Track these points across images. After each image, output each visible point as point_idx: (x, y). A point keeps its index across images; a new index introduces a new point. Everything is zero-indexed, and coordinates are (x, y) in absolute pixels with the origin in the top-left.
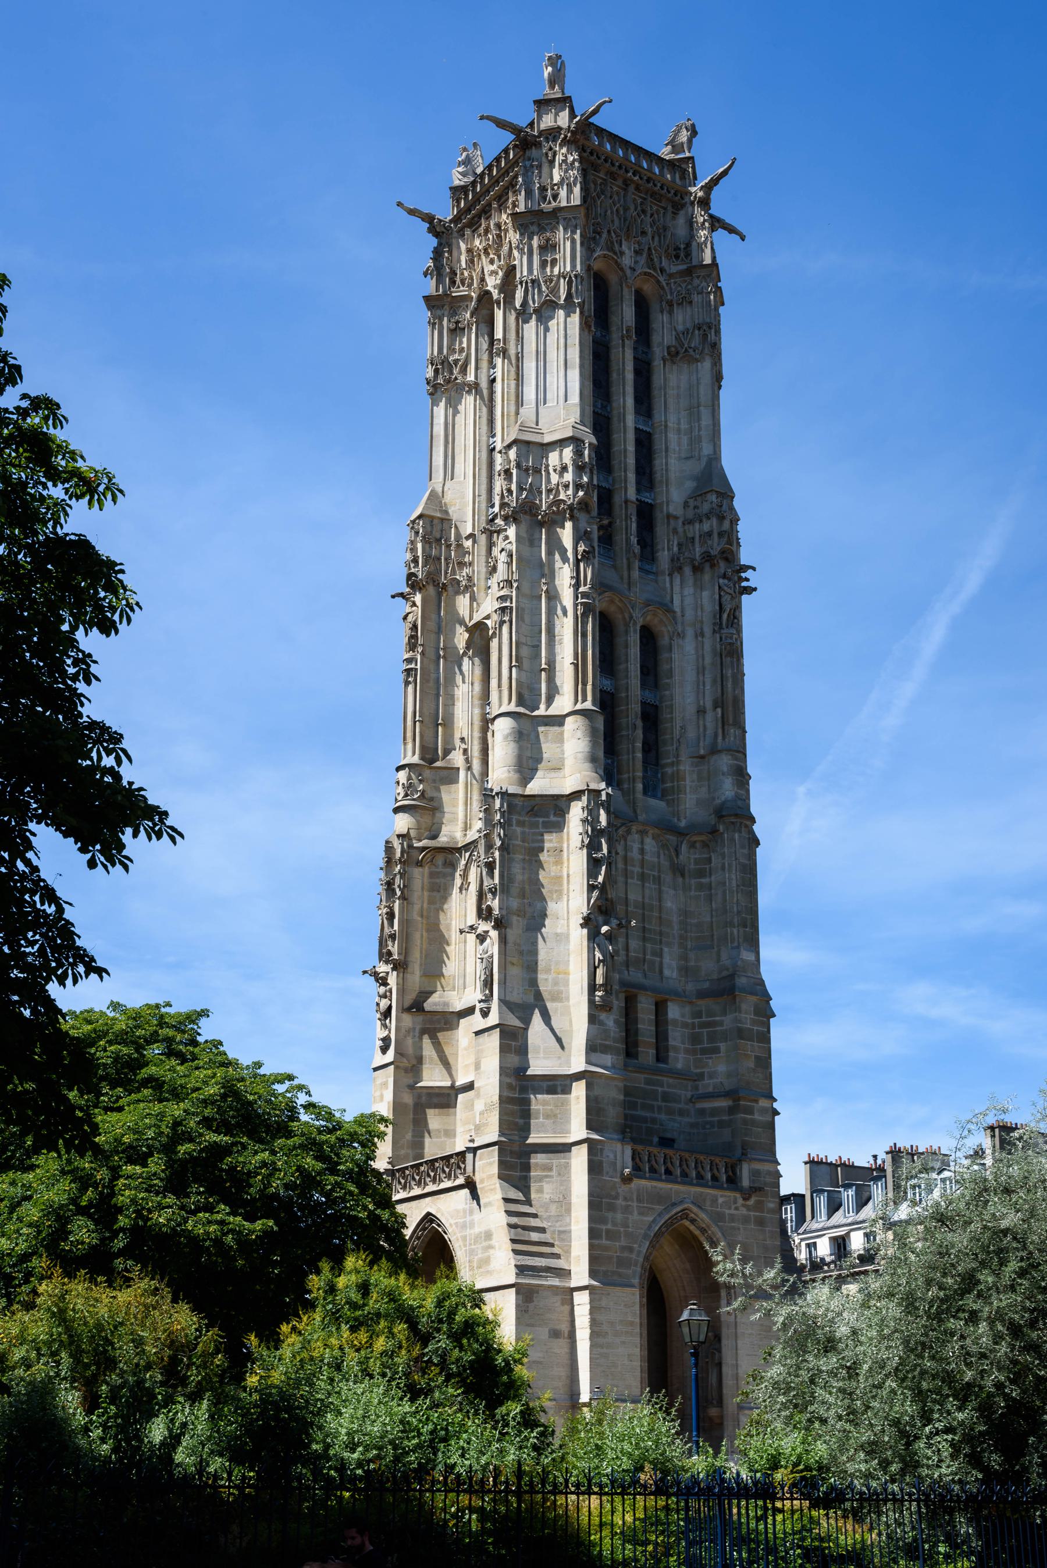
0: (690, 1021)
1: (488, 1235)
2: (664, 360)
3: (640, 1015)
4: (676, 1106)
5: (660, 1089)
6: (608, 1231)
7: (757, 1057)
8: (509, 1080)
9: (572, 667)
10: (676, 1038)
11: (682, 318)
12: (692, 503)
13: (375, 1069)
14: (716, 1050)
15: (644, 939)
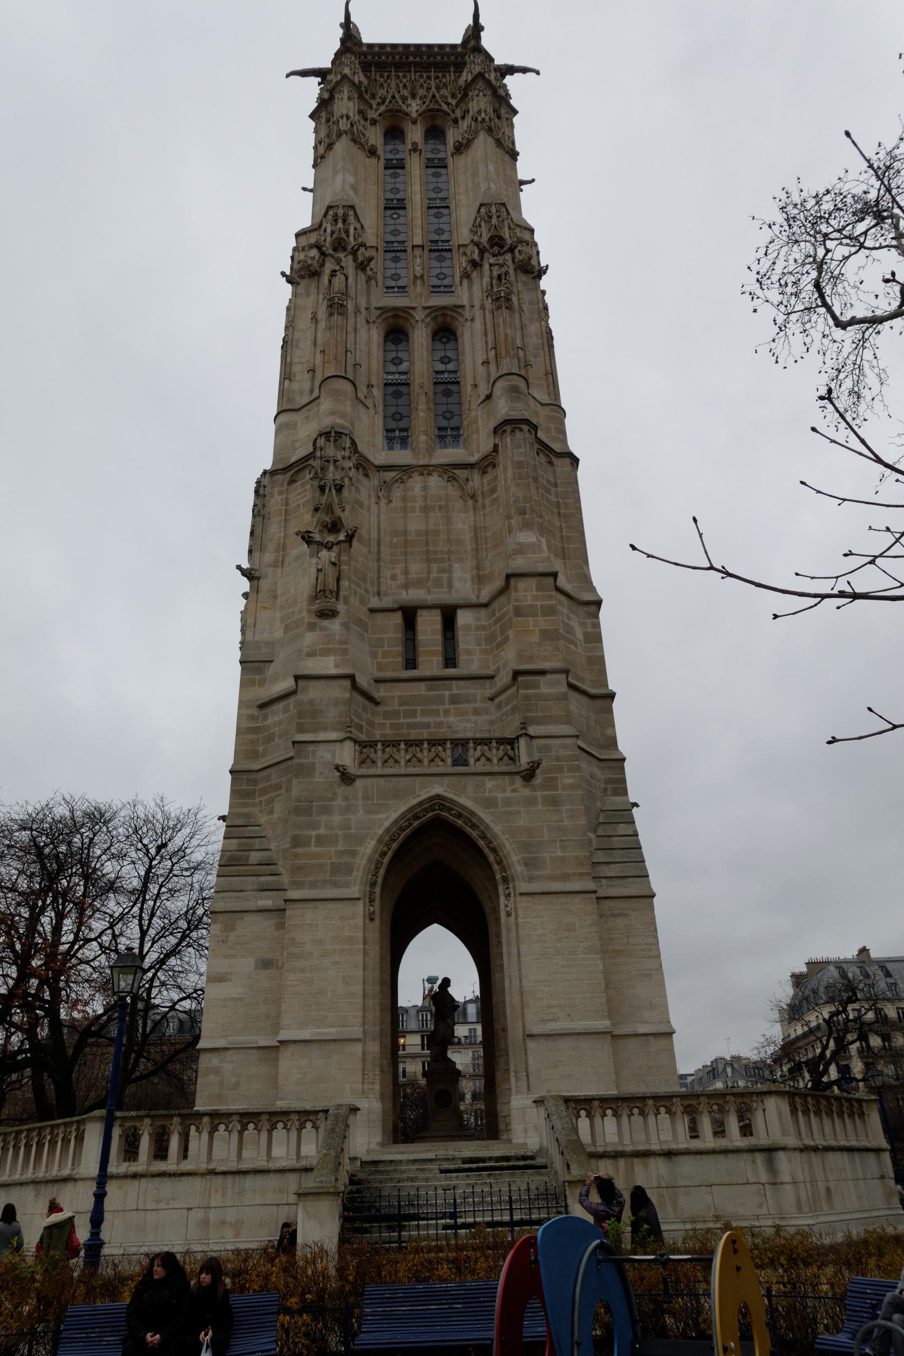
0: (486, 623)
2: (452, 155)
4: (470, 706)
5: (447, 693)
7: (540, 631)
8: (250, 712)
10: (466, 641)
14: (506, 640)
15: (428, 561)
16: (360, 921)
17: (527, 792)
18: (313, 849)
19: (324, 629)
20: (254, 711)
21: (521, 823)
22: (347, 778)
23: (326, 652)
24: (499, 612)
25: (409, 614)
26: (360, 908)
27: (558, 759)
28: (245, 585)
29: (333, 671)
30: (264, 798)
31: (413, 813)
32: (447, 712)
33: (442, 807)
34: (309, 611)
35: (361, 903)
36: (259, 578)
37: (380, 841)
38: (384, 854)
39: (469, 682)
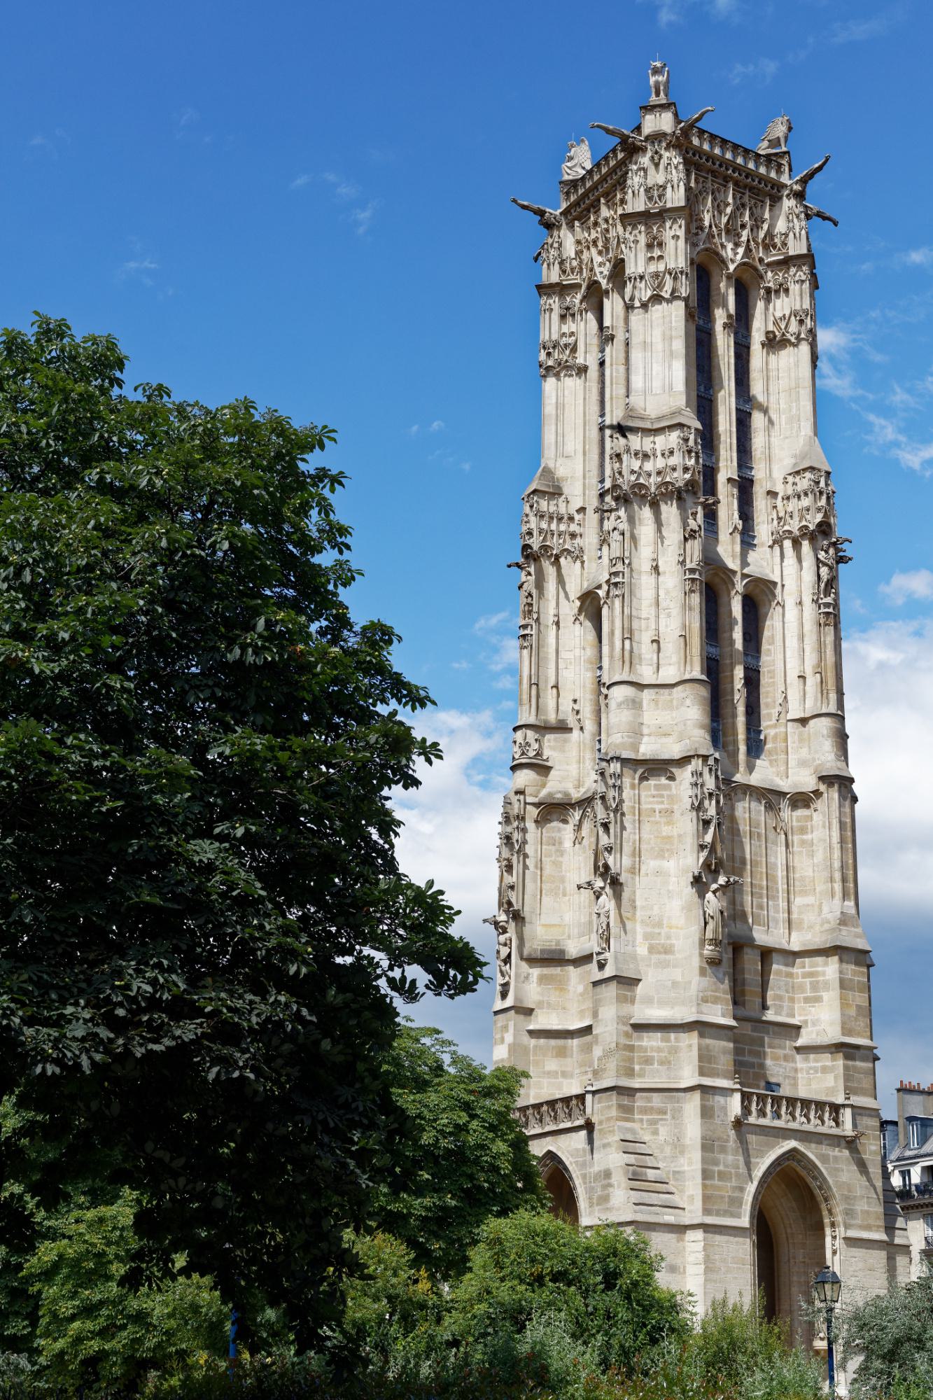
1: (607, 1174)
2: (763, 345)
3: (747, 966)
6: (720, 1173)
9: (682, 639)
11: (782, 306)
12: (790, 479)
13: (496, 1013)
14: (818, 999)
20: (629, 1029)
23: (716, 1000)
24: (811, 967)
30: (645, 1117)
34: (701, 955)
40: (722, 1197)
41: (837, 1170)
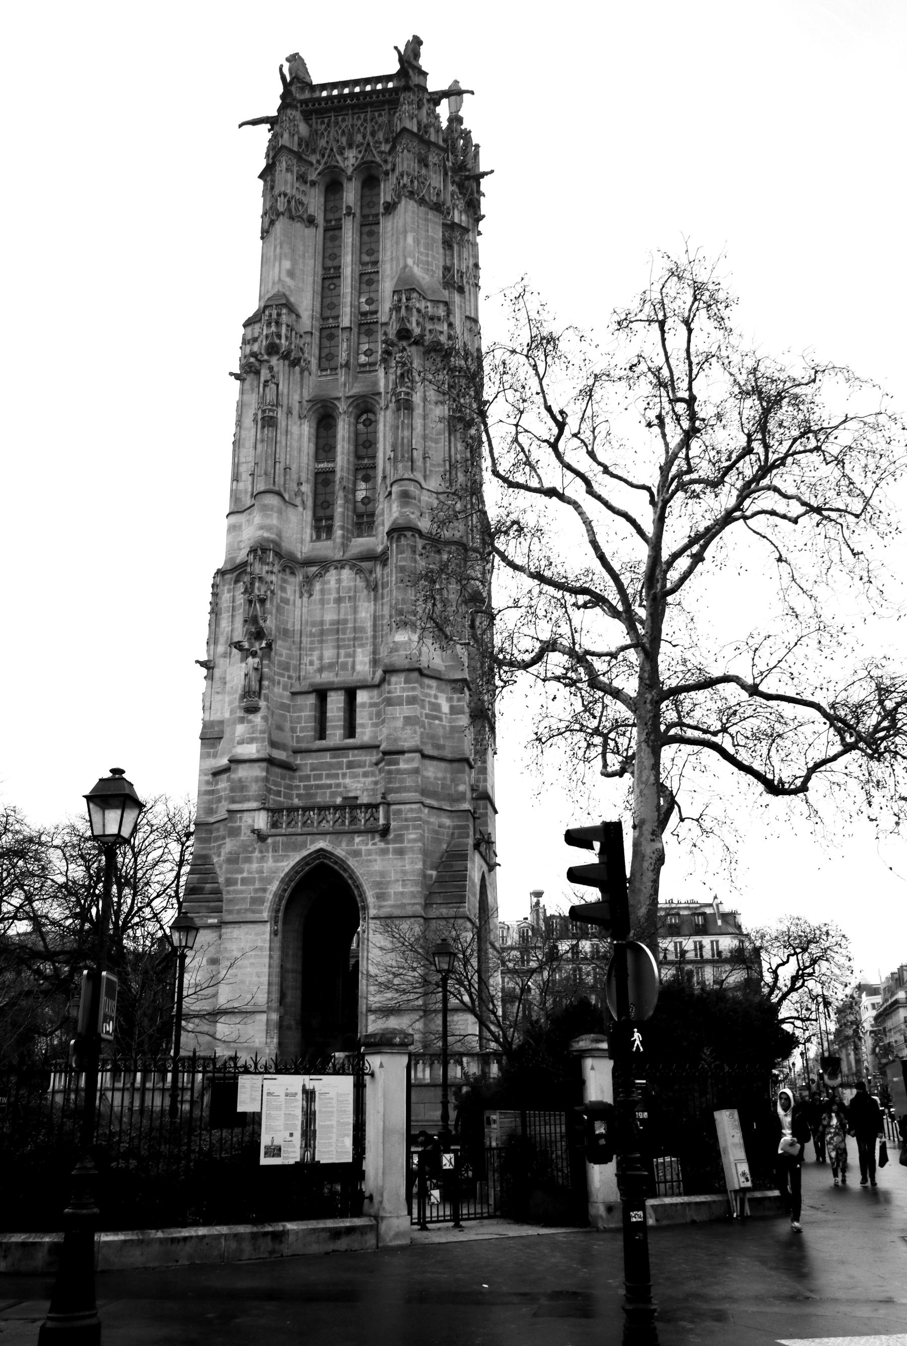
4: (360, 771)
5: (345, 760)
6: (243, 879)
8: (206, 778)
10: (362, 717)
16: (267, 936)
17: (382, 845)
18: (239, 887)
19: (249, 722)
20: (210, 778)
21: (376, 868)
22: (261, 837)
23: (251, 741)
25: (322, 694)
26: (267, 928)
27: (406, 820)
28: (204, 671)
29: (254, 756)
31: (305, 861)
32: (344, 775)
33: (326, 857)
34: (240, 707)
35: (268, 925)
36: (213, 668)
37: (282, 881)
38: (285, 890)
39: (361, 751)
40: (244, 899)
41: (370, 861)
